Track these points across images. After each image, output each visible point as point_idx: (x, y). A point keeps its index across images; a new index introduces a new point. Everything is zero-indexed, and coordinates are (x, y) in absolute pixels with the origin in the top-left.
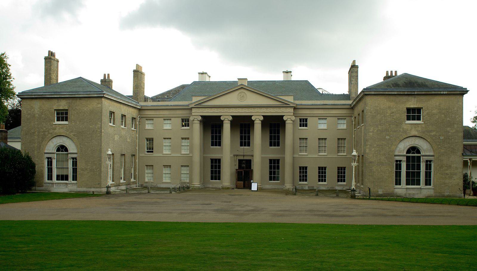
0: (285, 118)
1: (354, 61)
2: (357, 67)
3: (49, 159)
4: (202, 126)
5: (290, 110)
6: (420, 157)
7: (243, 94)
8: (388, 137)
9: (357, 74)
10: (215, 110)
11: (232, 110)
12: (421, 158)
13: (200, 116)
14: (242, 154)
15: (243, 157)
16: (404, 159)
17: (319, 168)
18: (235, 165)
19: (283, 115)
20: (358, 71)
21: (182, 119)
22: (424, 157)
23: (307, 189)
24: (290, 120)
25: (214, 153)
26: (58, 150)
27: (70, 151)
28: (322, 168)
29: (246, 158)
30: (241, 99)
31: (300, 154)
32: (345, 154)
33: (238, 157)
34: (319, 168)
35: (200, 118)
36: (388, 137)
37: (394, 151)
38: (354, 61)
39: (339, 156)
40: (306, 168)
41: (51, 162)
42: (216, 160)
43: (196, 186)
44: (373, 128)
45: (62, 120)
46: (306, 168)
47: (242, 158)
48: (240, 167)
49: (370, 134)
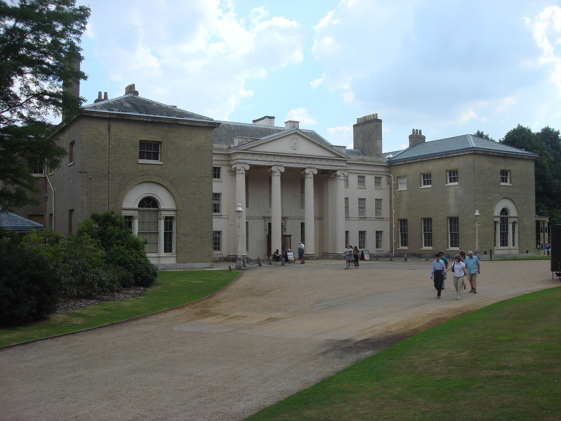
2: (380, 121)
3: (168, 220)
5: (343, 164)
6: (507, 218)
7: (295, 140)
8: (489, 198)
11: (283, 160)
12: (508, 218)
13: (249, 164)
16: (498, 220)
18: (266, 230)
22: (512, 219)
24: (343, 175)
26: (142, 204)
27: (162, 207)
30: (294, 147)
36: (489, 198)
37: (493, 212)
41: (171, 224)
45: (149, 158)
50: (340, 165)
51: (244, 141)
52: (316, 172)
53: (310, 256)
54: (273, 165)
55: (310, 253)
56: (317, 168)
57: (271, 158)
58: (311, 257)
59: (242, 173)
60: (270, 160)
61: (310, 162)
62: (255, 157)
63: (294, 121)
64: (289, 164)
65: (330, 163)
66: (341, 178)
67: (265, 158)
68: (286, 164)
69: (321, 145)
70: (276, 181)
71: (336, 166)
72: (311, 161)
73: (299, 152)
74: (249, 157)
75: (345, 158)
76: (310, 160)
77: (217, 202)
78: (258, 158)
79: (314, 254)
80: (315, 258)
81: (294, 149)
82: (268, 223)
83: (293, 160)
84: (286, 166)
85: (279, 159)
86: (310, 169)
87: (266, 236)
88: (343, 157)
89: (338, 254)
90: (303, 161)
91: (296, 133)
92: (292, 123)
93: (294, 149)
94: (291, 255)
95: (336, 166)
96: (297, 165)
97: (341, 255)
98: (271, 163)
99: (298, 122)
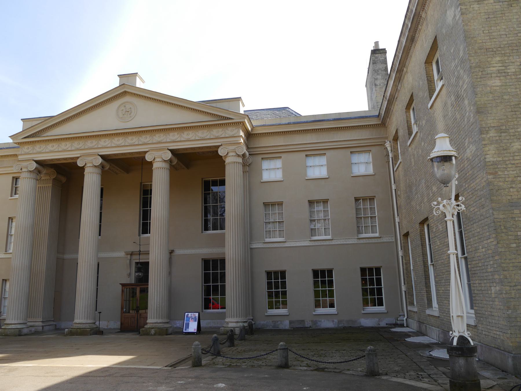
0: (221, 152)
1: (377, 43)
9: (386, 65)
10: (64, 145)
17: (316, 273)
18: (130, 275)
20: (386, 58)
21: (13, 177)
23: (287, 327)
24: (234, 154)
28: (323, 272)
31: (267, 240)
32: (377, 235)
34: (316, 273)
38: (377, 43)
39: (362, 241)
40: (283, 274)
43: (10, 327)
44: (498, 59)
46: (283, 274)
49: (490, 83)
50: (227, 136)
65: (201, 134)
74: (38, 148)
88: (230, 119)
90: (145, 139)
91: (125, 93)
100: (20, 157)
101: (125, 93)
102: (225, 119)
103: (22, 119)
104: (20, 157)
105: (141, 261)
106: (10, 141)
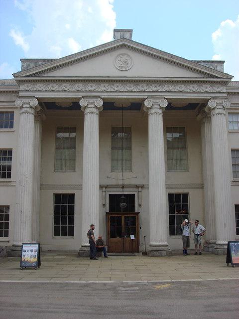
4: (39, 125)
7: (124, 58)
11: (102, 87)
13: (37, 98)
14: (120, 183)
15: (121, 189)
18: (104, 206)
19: (205, 98)
25: (63, 182)
29: (127, 192)
33: (107, 190)
35: (36, 103)
42: (65, 196)
47: (118, 192)
48: (112, 208)
51: (31, 66)
52: (165, 104)
53: (155, 249)
54: (81, 96)
55: (157, 244)
56: (166, 97)
57: (80, 87)
58: (156, 251)
59: (28, 113)
60: (77, 88)
61: (153, 88)
62: (50, 87)
63: (122, 30)
64: (111, 94)
65: (194, 88)
66: (216, 111)
67: (67, 87)
68: (106, 94)
69: (173, 60)
70: (91, 123)
71: (206, 92)
72: (156, 87)
73: (130, 74)
74: (38, 87)
75: (224, 78)
76: (153, 85)
77: (6, 163)
78: (56, 87)
79: (167, 246)
80: (164, 253)
81: (122, 71)
82: (109, 195)
83: (121, 88)
84: (106, 97)
85: (94, 87)
86: (152, 100)
87: (104, 213)
89: (218, 246)
91: (124, 46)
92: (119, 33)
93: (122, 71)
94: (32, 251)
95: (206, 92)
96: (127, 94)
97: (222, 248)
98: (77, 94)
99: (130, 31)
100: (21, 94)
101: (124, 46)
102: (213, 78)
103: (21, 60)
104: (21, 94)
105: (124, 193)
106: (12, 77)
